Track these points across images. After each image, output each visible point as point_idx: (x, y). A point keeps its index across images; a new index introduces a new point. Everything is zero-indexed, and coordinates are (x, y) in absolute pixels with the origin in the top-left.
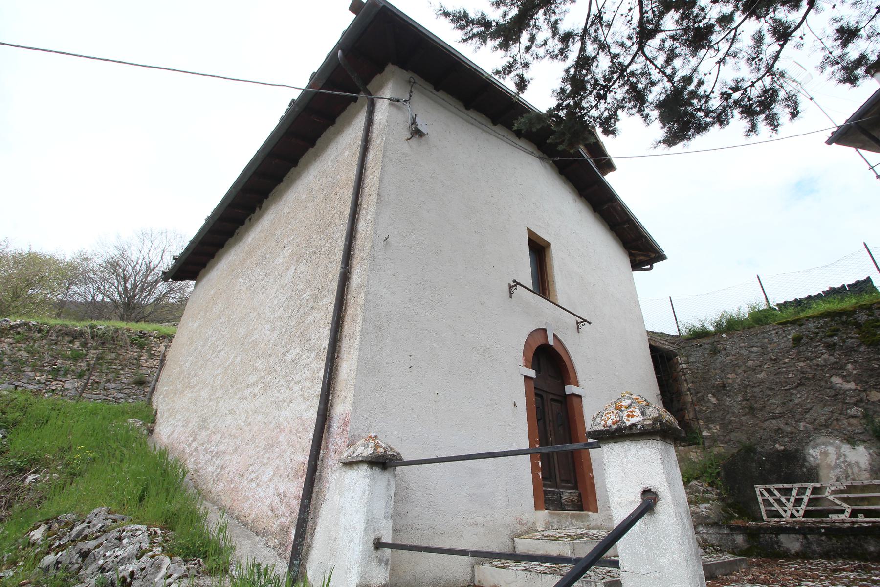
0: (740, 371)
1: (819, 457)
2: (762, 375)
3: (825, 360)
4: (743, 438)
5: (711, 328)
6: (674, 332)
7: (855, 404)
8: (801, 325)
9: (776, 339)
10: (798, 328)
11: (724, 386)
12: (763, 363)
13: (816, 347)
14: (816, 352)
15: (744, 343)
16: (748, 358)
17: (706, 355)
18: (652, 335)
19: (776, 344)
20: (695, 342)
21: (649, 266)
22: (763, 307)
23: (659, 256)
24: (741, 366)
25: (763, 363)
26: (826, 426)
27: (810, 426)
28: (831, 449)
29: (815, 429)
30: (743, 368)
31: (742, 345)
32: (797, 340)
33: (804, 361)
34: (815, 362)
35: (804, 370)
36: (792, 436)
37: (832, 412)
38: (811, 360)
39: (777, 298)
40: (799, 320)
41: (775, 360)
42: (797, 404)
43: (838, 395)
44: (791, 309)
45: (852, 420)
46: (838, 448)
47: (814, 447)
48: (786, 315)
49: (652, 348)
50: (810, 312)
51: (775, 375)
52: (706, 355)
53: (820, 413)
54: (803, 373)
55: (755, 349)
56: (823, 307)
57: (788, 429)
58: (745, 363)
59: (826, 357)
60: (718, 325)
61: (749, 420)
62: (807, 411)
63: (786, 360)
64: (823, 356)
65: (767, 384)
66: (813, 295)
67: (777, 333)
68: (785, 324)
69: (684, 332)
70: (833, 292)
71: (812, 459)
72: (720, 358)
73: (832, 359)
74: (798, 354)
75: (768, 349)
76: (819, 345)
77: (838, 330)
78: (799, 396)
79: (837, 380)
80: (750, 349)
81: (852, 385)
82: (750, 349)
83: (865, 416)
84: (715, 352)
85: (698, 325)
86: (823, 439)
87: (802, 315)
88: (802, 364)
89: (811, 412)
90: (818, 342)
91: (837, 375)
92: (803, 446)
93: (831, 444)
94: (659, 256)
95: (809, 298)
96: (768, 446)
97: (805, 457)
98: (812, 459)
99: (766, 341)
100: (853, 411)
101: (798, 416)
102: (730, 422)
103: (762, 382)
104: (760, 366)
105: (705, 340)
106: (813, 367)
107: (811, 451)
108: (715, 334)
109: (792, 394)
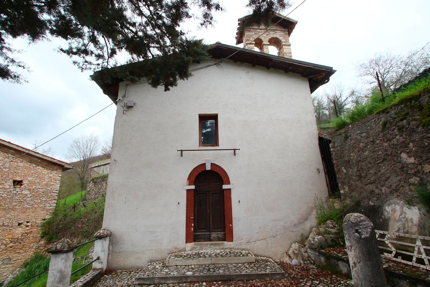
1: (390, 212)
2: (367, 153)
3: (398, 140)
8: (387, 113)
9: (374, 126)
10: (386, 115)
13: (393, 130)
14: (392, 134)
15: (359, 130)
16: (360, 141)
17: (342, 141)
19: (374, 130)
24: (357, 147)
25: (367, 144)
26: (396, 190)
27: (388, 190)
28: (398, 208)
29: (391, 192)
30: (358, 149)
31: (358, 132)
32: (385, 124)
33: (386, 142)
34: (392, 142)
35: (386, 149)
37: (400, 180)
38: (390, 141)
40: (386, 109)
41: (373, 141)
42: (382, 174)
43: (404, 167)
47: (389, 205)
51: (373, 152)
52: (342, 141)
53: (394, 180)
54: (386, 151)
55: (364, 134)
58: (359, 145)
59: (399, 138)
63: (378, 142)
64: (397, 137)
67: (375, 121)
71: (386, 213)
72: (348, 142)
73: (402, 139)
74: (383, 136)
75: (370, 134)
76: (395, 128)
78: (384, 167)
80: (361, 135)
81: (412, 160)
82: (361, 135)
86: (395, 200)
88: (386, 144)
89: (389, 179)
90: (394, 126)
91: (404, 152)
92: (383, 204)
93: (398, 204)
97: (383, 211)
98: (386, 213)
99: (369, 127)
101: (382, 183)
104: (365, 147)
106: (391, 146)
107: (387, 208)
109: (380, 166)
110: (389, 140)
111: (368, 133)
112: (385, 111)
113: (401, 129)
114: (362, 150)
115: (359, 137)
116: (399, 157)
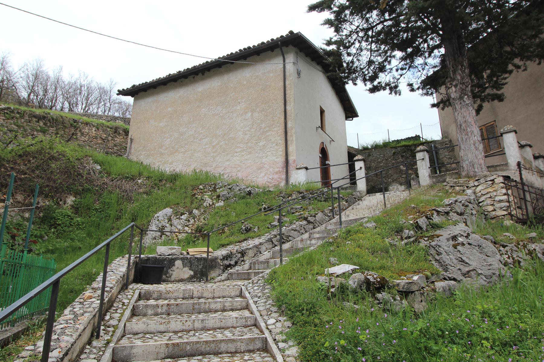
0: (376, 162)
2: (382, 164)
4: (373, 184)
5: (370, 147)
6: (357, 147)
7: (405, 174)
11: (370, 167)
12: (383, 160)
18: (350, 148)
20: (363, 152)
21: (351, 119)
22: (387, 141)
23: (357, 116)
25: (383, 160)
32: (394, 153)
36: (386, 183)
38: (396, 160)
39: (393, 138)
43: (401, 171)
44: (395, 143)
45: (403, 179)
46: (397, 186)
48: (393, 145)
49: (348, 152)
50: (400, 145)
53: (395, 176)
56: (404, 143)
57: (385, 181)
60: (372, 146)
61: (375, 178)
62: (392, 176)
65: (383, 167)
66: (403, 138)
68: (392, 148)
69: (361, 148)
70: (409, 139)
74: (393, 158)
77: (406, 151)
79: (402, 167)
83: (406, 177)
84: (369, 155)
85: (365, 145)
87: (398, 145)
91: (402, 165)
94: (357, 116)
95: (402, 140)
96: (379, 186)
100: (403, 176)
102: (370, 179)
103: (381, 166)
105: (367, 151)
107: (390, 187)
108: (371, 149)
110: (396, 160)
111: (384, 155)
112: (395, 148)
113: (402, 156)
114: (380, 162)
115: (379, 156)
116: (399, 166)
